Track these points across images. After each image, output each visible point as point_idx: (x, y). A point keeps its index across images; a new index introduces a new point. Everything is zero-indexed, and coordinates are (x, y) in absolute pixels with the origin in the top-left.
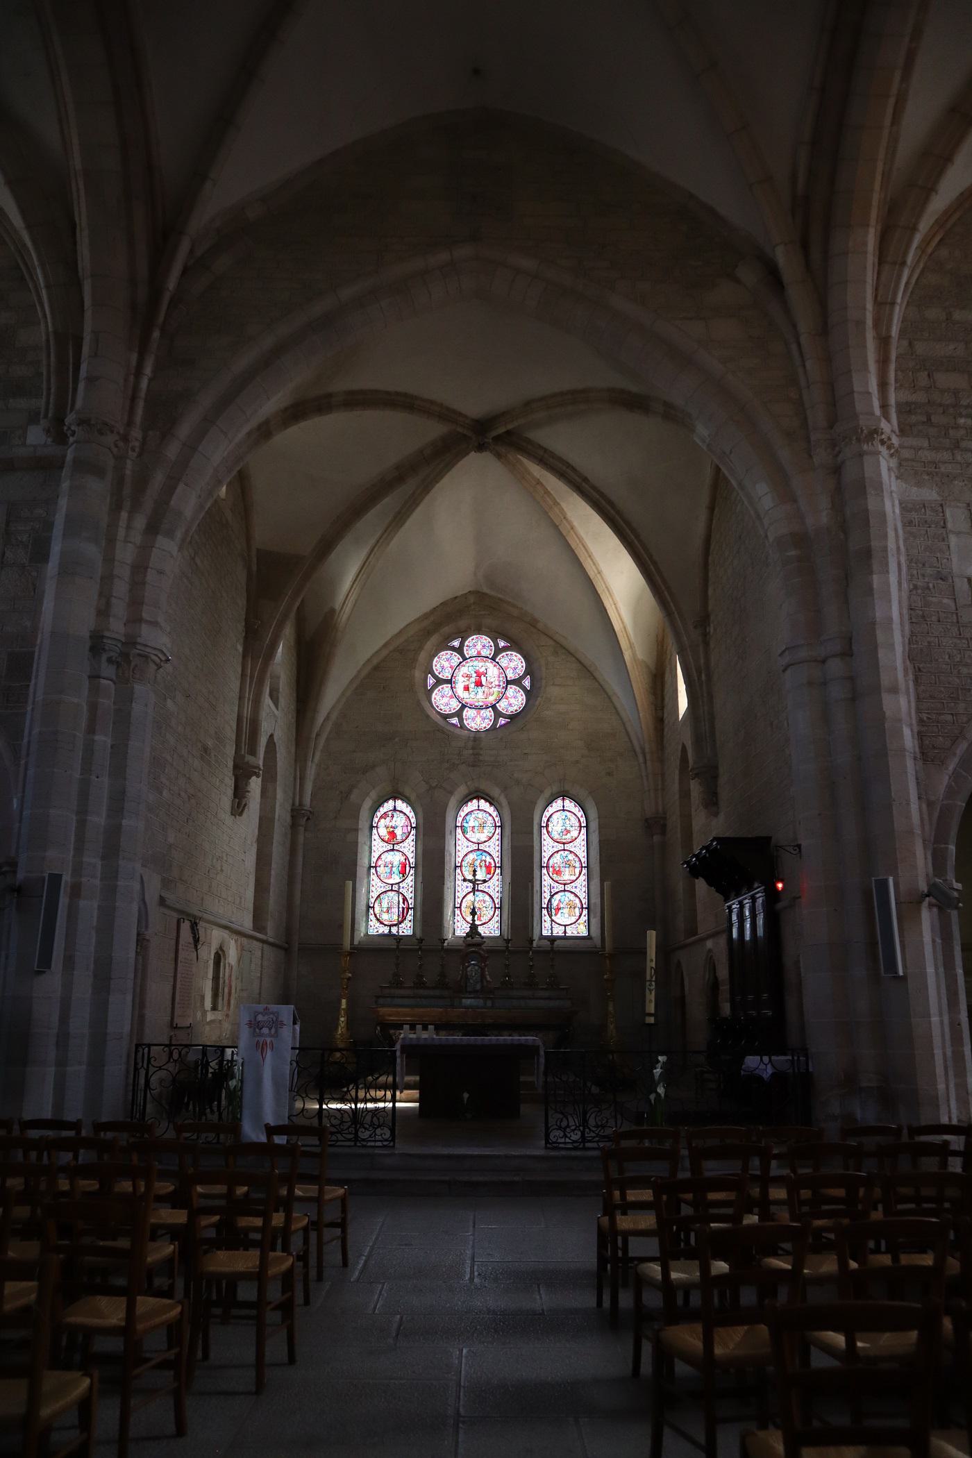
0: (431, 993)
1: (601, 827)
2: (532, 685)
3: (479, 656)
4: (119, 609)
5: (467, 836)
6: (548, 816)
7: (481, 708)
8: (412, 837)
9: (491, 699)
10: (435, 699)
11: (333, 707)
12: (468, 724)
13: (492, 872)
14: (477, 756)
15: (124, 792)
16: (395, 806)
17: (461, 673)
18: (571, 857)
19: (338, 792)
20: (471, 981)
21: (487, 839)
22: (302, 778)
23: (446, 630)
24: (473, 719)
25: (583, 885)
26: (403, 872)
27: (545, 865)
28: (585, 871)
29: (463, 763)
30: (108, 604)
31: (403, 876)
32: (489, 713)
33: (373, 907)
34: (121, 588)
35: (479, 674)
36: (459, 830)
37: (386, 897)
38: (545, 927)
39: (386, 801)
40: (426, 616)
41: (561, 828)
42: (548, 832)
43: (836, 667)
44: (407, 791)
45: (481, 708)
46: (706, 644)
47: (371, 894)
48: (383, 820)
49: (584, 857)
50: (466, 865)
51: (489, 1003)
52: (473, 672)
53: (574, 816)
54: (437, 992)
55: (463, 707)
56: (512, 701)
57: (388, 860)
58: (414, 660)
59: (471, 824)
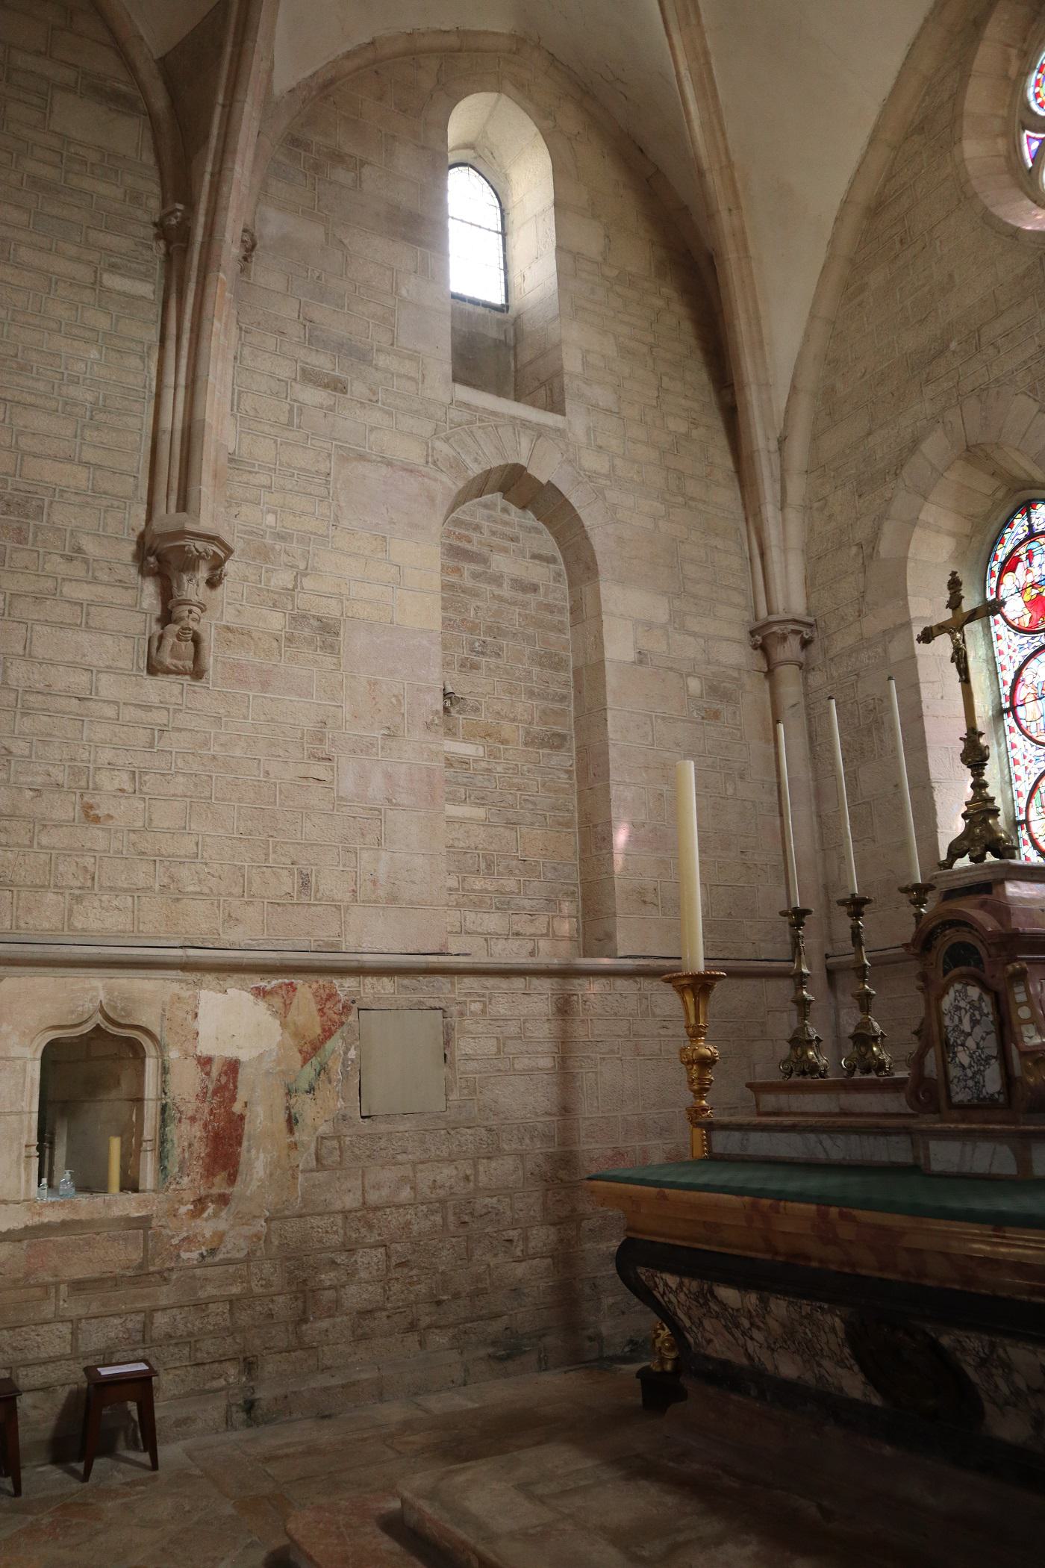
11: (800, 357)
16: (1030, 526)
19: (854, 550)
20: (963, 1058)
33: (1027, 822)
39: (1008, 523)
47: (1016, 785)
48: (1008, 578)
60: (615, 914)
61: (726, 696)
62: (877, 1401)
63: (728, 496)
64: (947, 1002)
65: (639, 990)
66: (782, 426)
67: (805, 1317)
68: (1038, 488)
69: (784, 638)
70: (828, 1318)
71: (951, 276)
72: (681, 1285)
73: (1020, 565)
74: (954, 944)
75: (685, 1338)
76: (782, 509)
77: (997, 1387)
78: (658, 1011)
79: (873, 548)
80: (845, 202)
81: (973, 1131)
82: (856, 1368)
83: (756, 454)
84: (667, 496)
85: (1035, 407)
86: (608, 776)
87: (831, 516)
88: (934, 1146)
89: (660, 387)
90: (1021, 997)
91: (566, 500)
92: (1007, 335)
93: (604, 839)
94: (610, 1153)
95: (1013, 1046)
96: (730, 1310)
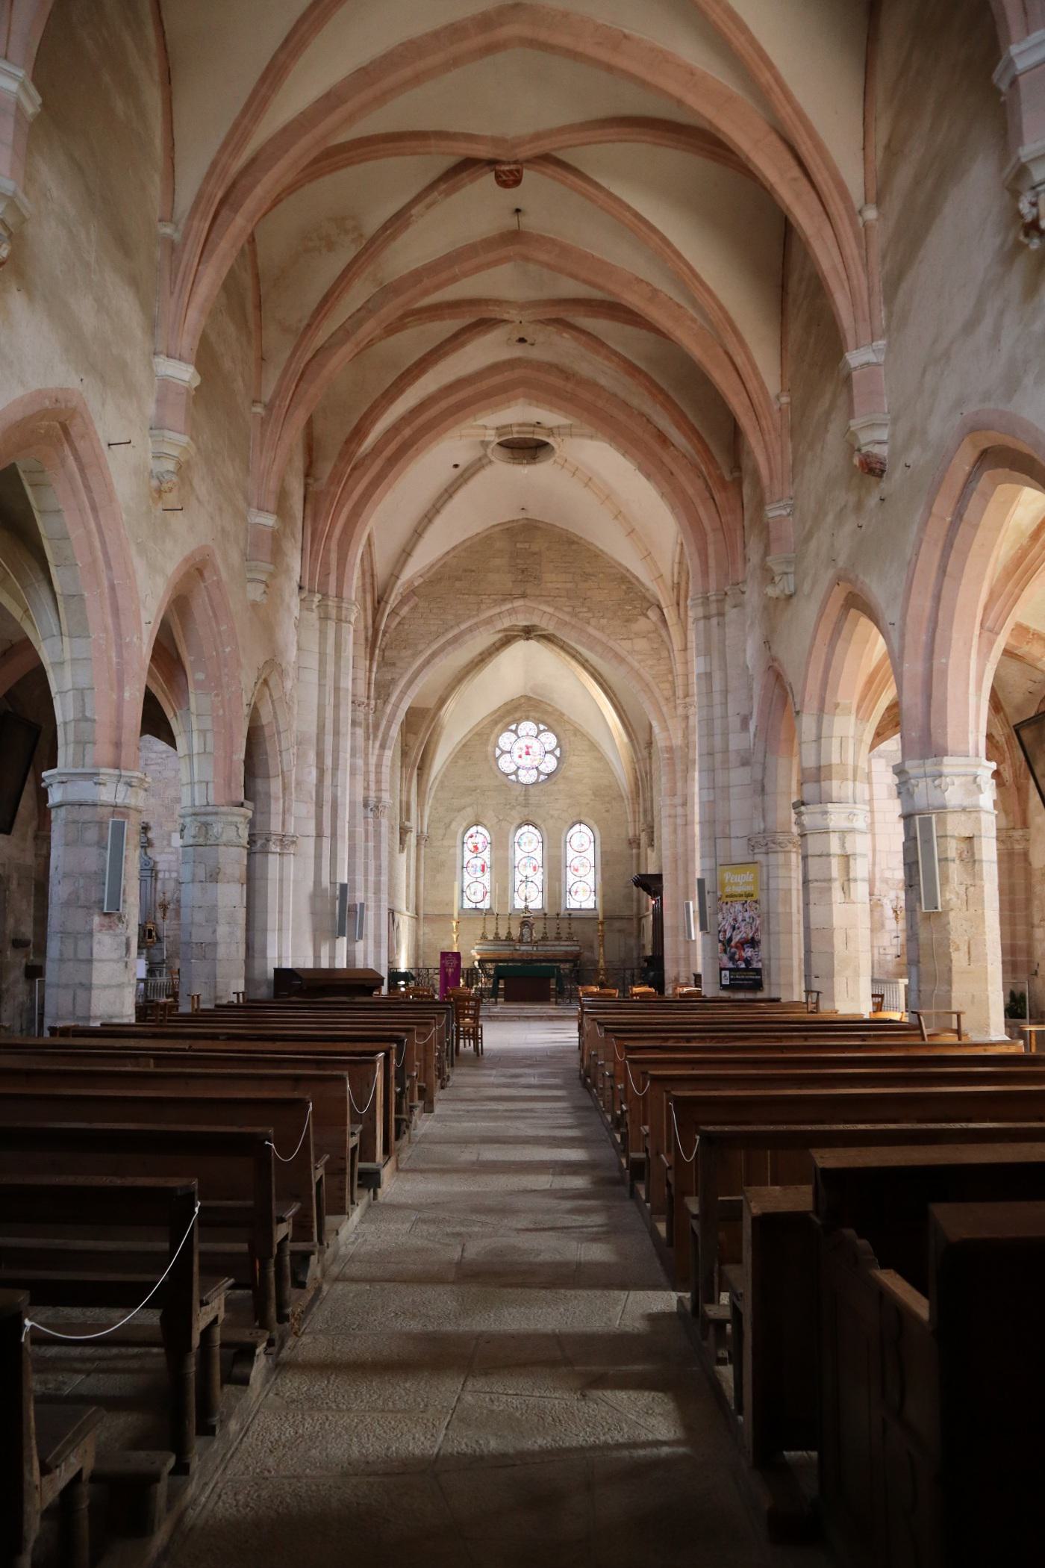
0: (504, 943)
1: (602, 843)
2: (561, 754)
3: (527, 735)
4: (372, 786)
8: (488, 849)
9: (536, 764)
11: (440, 771)
15: (380, 866)
18: (585, 861)
22: (422, 816)
23: (507, 720)
26: (483, 870)
30: (368, 785)
32: (535, 772)
34: (372, 777)
35: (528, 747)
36: (516, 845)
40: (495, 712)
43: (680, 810)
44: (485, 822)
46: (650, 758)
51: (535, 949)
54: (506, 943)
55: (518, 768)
58: (488, 740)
80: (460, 742)
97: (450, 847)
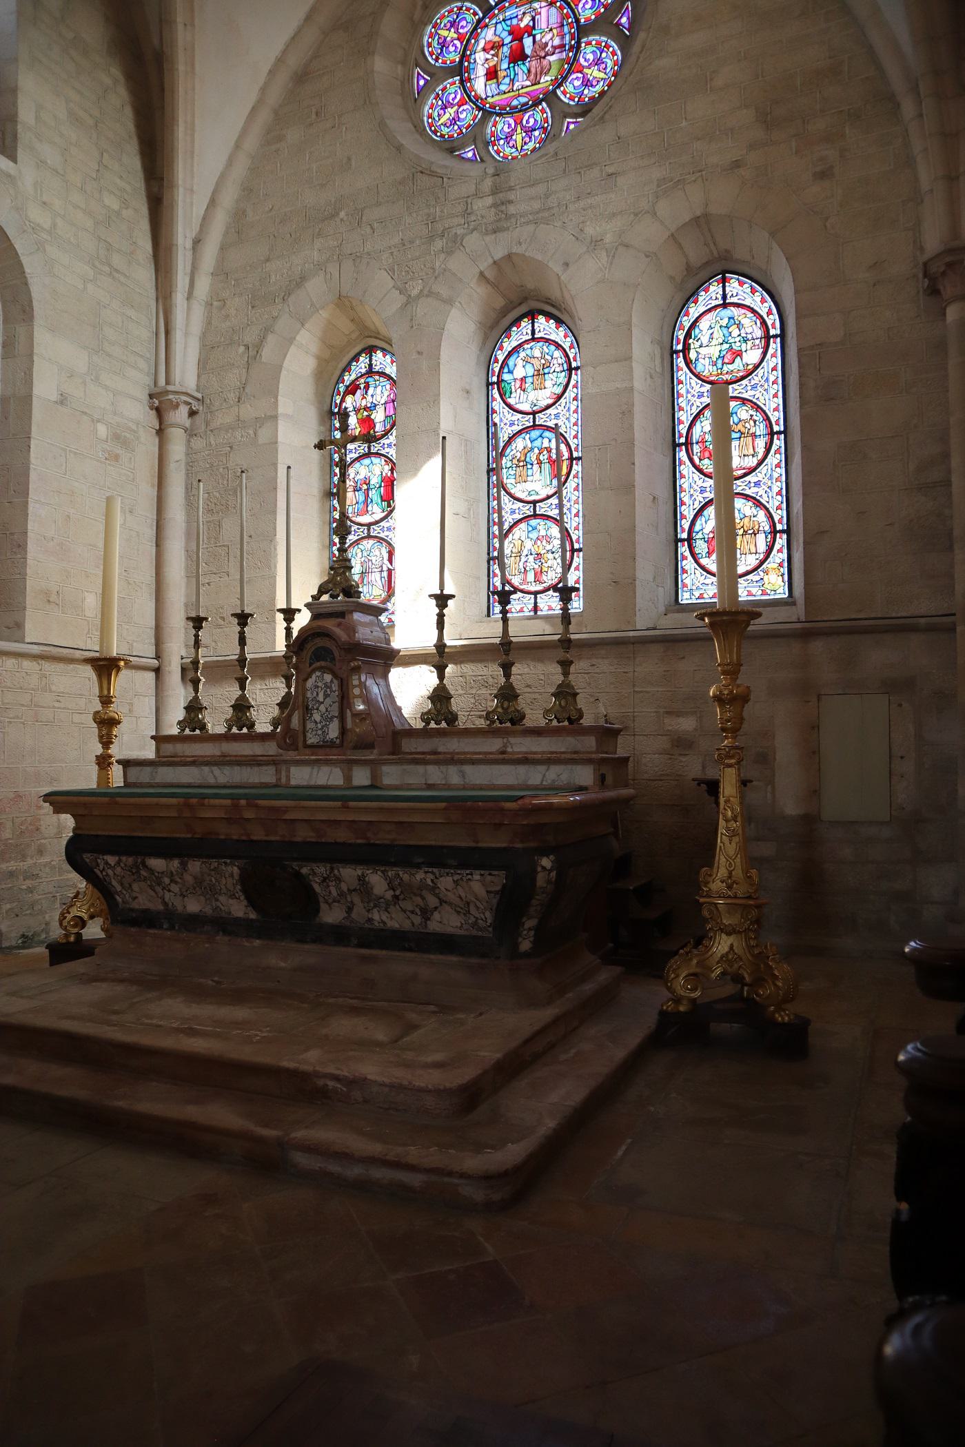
5: (511, 401)
6: (687, 325)
7: (524, 108)
10: (430, 116)
11: (222, 177)
12: (498, 152)
13: (564, 471)
14: (503, 208)
16: (371, 365)
17: (482, 44)
19: (242, 349)
20: (317, 717)
21: (551, 401)
24: (508, 138)
25: (776, 475)
27: (683, 440)
28: (778, 442)
29: (475, 229)
31: (389, 506)
35: (517, 34)
37: (359, 551)
38: (685, 585)
39: (356, 358)
41: (719, 348)
42: (688, 363)
45: (524, 108)
48: (349, 399)
49: (776, 409)
50: (509, 464)
52: (504, 34)
53: (750, 315)
56: (594, 73)
57: (361, 476)
59: (519, 372)
60: (24, 608)
61: (125, 444)
62: (253, 916)
63: (144, 275)
64: (310, 683)
65: (41, 670)
66: (198, 229)
67: (213, 870)
68: (381, 339)
69: (177, 406)
70: (229, 869)
71: (349, 159)
72: (118, 863)
73: (359, 391)
74: (319, 648)
75: (116, 899)
76: (188, 299)
77: (330, 892)
78: (54, 688)
79: (257, 352)
80: (280, 61)
81: (321, 760)
82: (242, 898)
83: (174, 248)
84: (97, 263)
85: (391, 283)
86: (28, 494)
87: (228, 316)
88: (293, 770)
89: (100, 163)
90: (356, 682)
91: (12, 244)
92: (382, 222)
93: (20, 546)
94: (12, 795)
95: (348, 711)
96: (156, 874)
97: (260, 422)
